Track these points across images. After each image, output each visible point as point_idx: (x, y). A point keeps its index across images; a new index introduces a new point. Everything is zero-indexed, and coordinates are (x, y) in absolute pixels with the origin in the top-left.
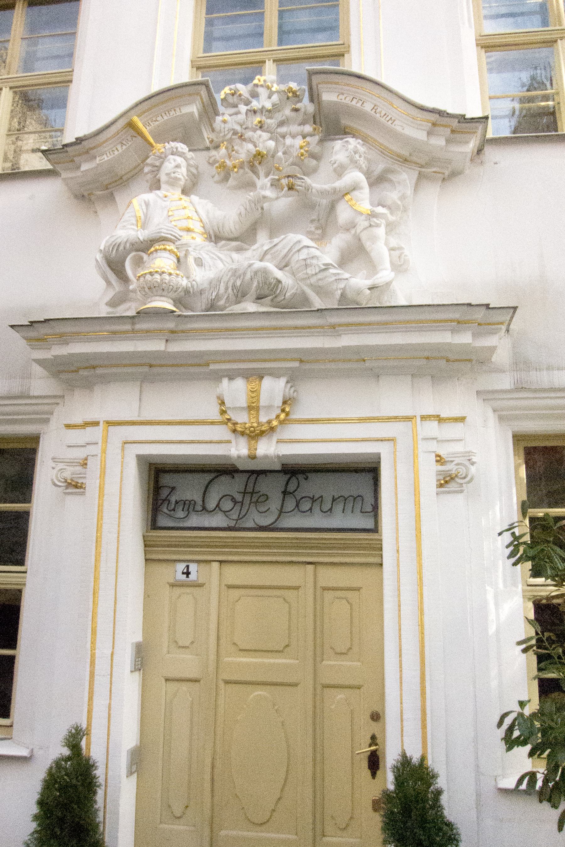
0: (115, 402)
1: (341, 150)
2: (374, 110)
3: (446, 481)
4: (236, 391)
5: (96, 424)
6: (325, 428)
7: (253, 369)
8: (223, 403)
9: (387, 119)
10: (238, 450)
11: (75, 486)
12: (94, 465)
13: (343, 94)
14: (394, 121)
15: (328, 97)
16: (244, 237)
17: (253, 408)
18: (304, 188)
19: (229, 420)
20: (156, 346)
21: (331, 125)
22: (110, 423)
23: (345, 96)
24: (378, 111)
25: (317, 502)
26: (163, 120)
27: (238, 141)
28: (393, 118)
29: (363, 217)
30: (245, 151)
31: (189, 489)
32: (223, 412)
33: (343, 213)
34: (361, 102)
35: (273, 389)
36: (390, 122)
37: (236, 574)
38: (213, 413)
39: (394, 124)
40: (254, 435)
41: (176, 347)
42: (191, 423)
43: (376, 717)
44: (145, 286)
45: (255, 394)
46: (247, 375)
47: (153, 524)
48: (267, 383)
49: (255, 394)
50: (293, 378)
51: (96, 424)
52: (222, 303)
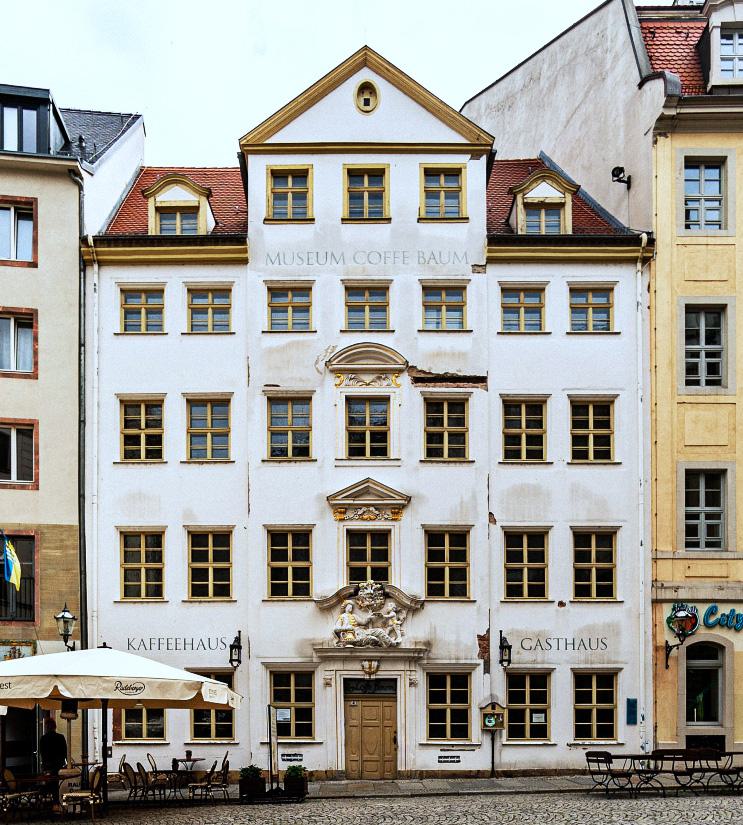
0: (338, 666)
1: (390, 605)
3: (411, 684)
4: (366, 664)
6: (386, 672)
10: (367, 677)
11: (328, 684)
12: (333, 680)
15: (387, 590)
16: (366, 626)
17: (370, 667)
20: (348, 654)
21: (387, 596)
25: (385, 689)
30: (367, 603)
31: (353, 684)
33: (390, 623)
37: (365, 703)
38: (360, 668)
40: (370, 674)
42: (355, 671)
43: (396, 732)
45: (370, 666)
46: (369, 661)
47: (345, 692)
49: (370, 666)
50: (378, 661)
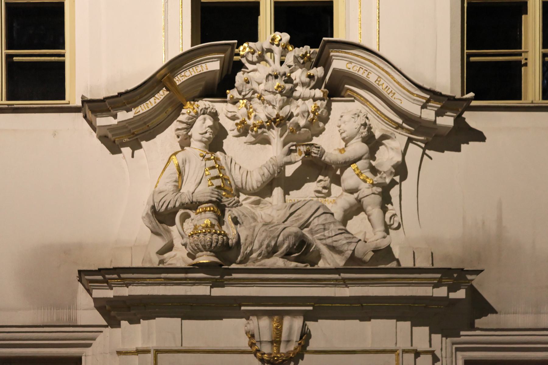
2: (377, 82)
4: (264, 326)
5: (147, 351)
7: (276, 308)
8: (253, 336)
9: (389, 92)
13: (351, 63)
14: (394, 94)
18: (318, 156)
19: (258, 351)
20: (203, 290)
22: (158, 352)
23: (353, 64)
24: (380, 83)
26: (191, 76)
27: (257, 100)
28: (393, 91)
29: (367, 185)
32: (252, 345)
34: (366, 73)
35: (293, 326)
36: (391, 95)
39: (394, 97)
41: (217, 292)
44: (199, 244)
48: (287, 321)
51: (147, 351)
52: (254, 255)
